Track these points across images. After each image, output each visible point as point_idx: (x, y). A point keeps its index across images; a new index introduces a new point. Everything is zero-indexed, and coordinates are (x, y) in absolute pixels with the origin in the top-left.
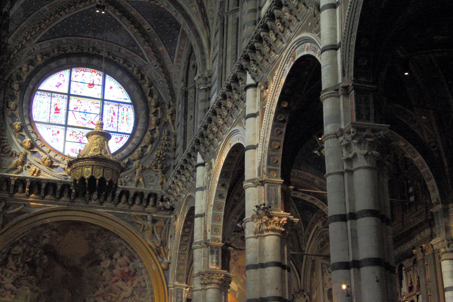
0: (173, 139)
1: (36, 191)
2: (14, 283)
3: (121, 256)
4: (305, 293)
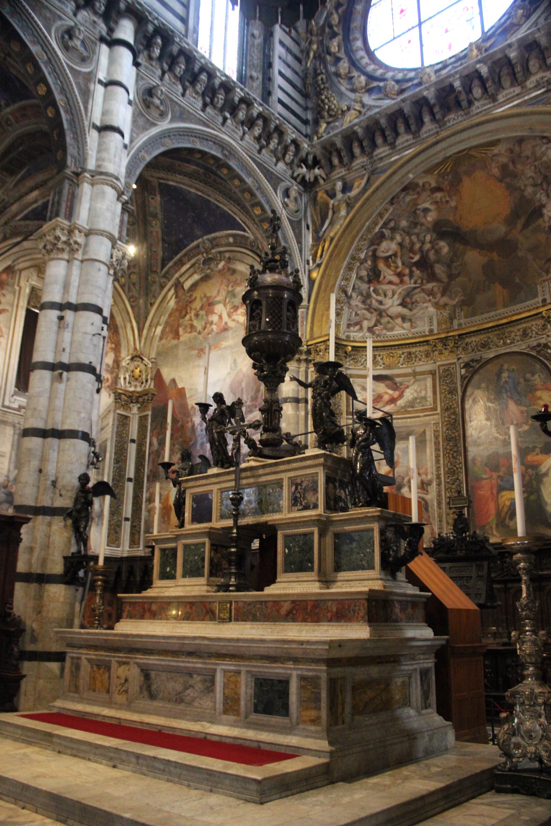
2: (403, 304)
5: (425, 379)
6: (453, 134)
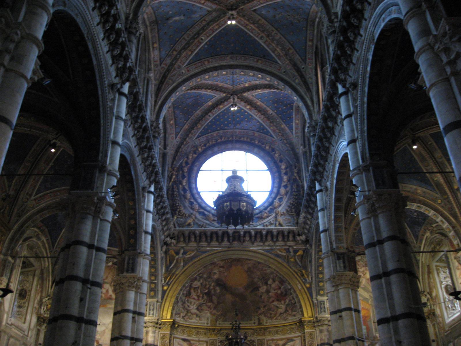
0: (301, 190)
1: (204, 239)
3: (274, 281)
4: (426, 293)
5: (203, 344)
6: (235, 250)
